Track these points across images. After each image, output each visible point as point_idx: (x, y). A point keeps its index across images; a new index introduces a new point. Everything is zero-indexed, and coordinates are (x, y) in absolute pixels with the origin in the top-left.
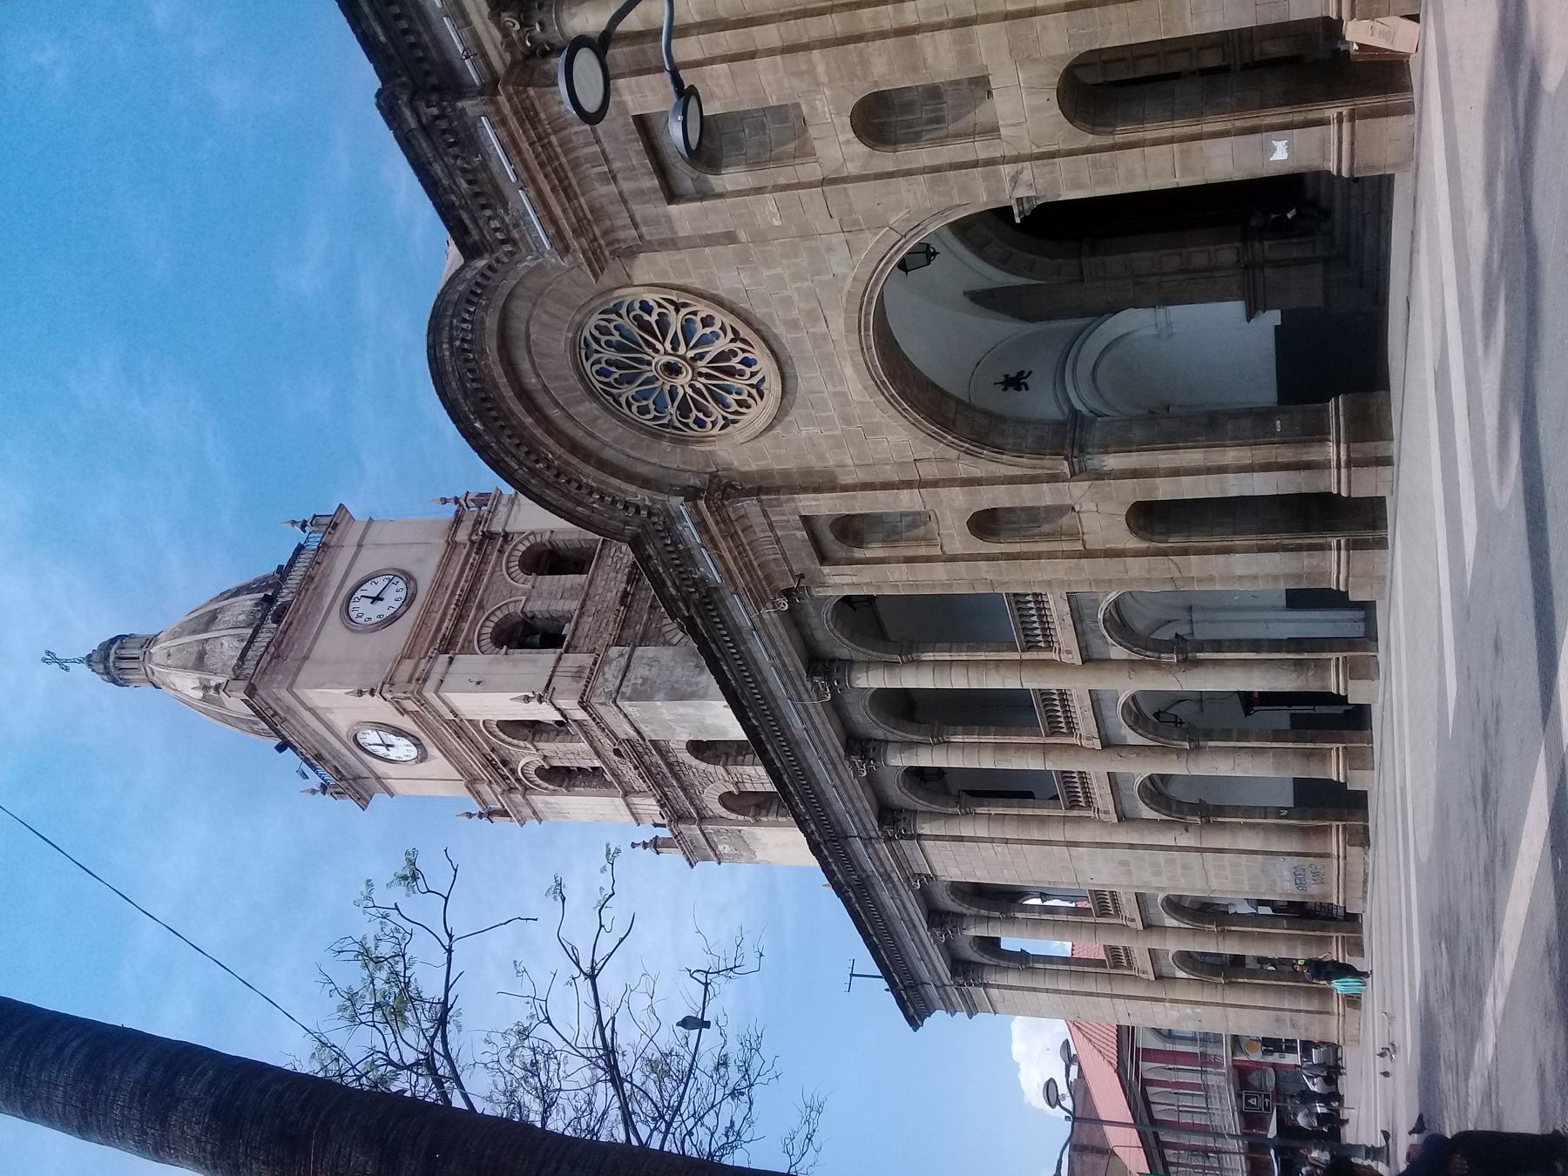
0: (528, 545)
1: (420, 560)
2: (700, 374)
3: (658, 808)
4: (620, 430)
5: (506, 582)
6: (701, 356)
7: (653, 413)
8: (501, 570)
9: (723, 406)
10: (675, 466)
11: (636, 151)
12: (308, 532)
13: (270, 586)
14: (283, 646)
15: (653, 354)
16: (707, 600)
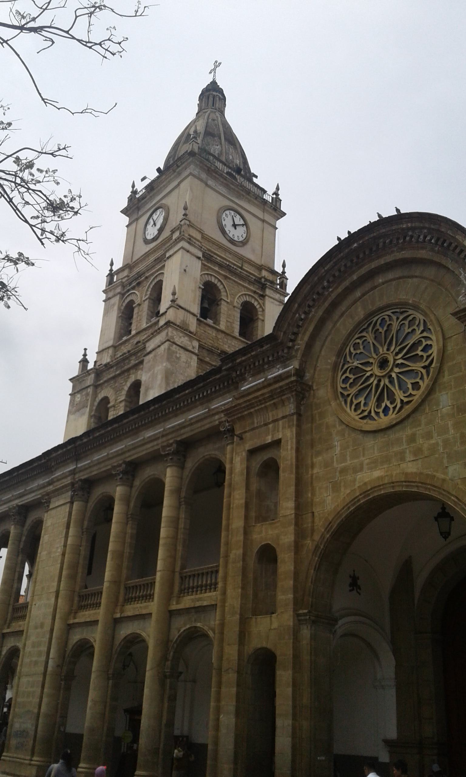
0: (258, 307)
2: (379, 381)
3: (104, 362)
5: (238, 293)
6: (391, 381)
7: (354, 352)
9: (357, 395)
10: (318, 365)
12: (273, 196)
13: (246, 174)
15: (394, 353)
16: (230, 382)
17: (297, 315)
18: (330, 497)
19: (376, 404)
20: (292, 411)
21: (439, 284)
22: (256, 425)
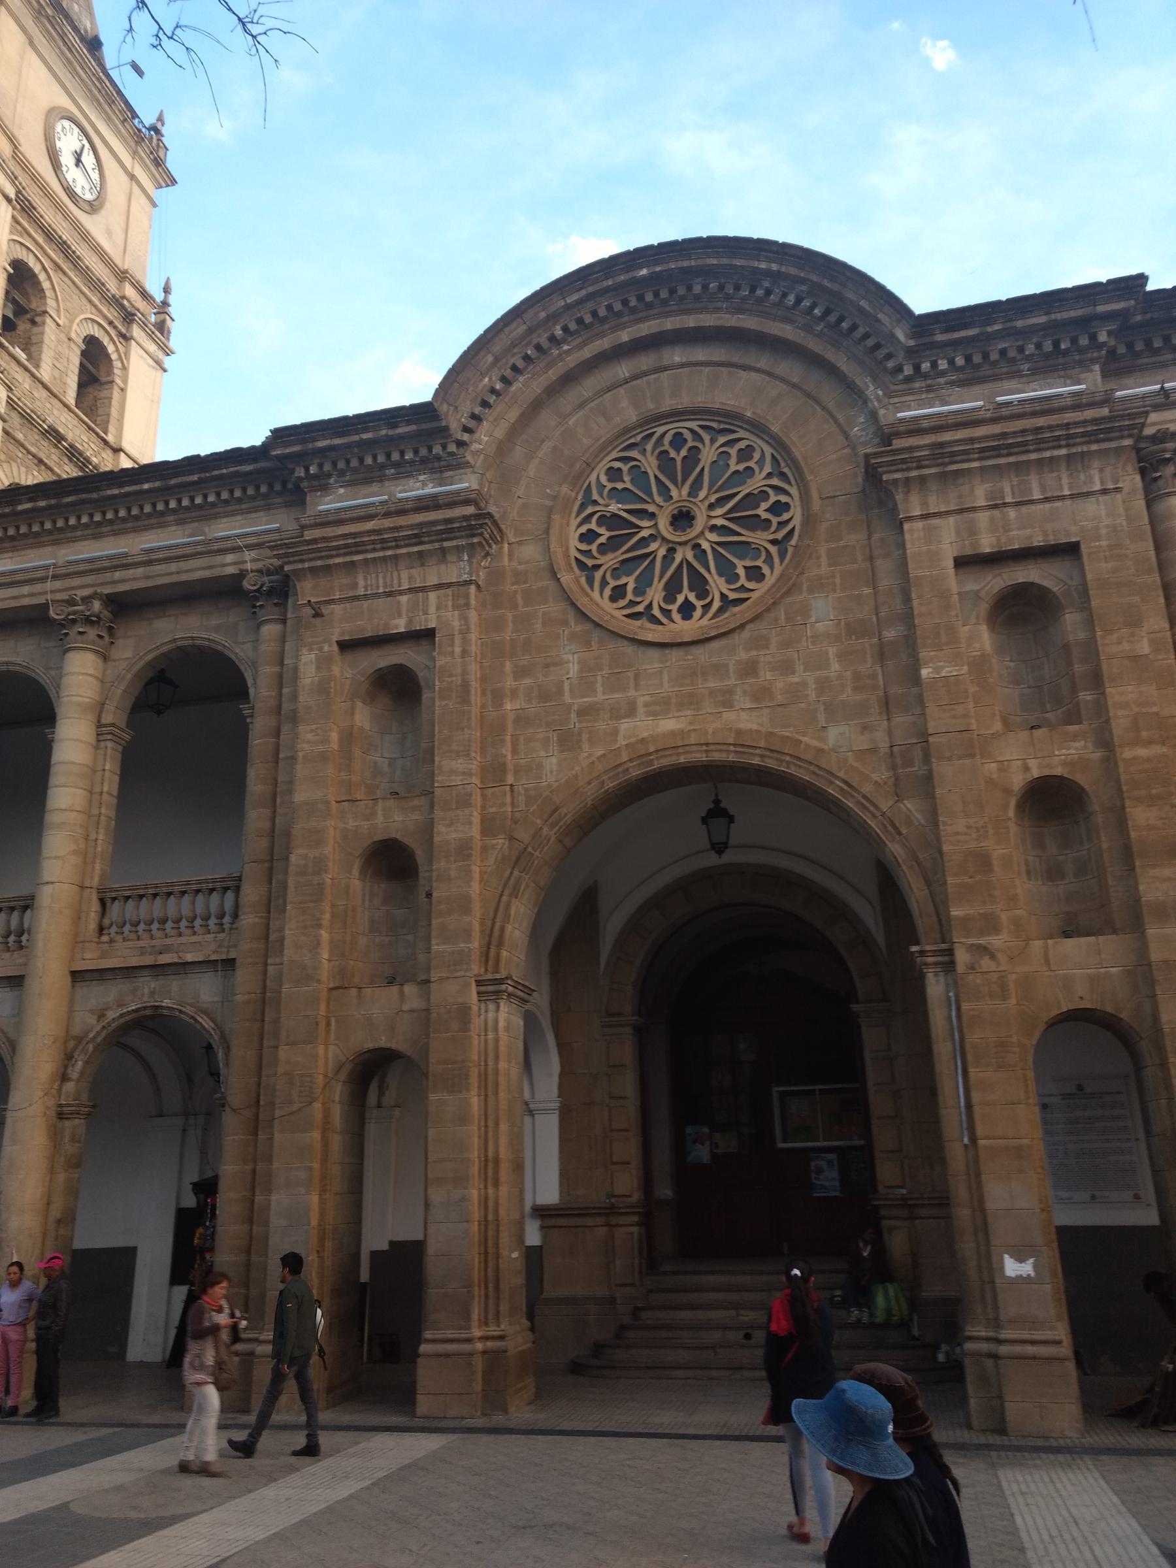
0: (114, 356)
1: (109, 232)
2: (672, 551)
4: (587, 442)
8: (92, 313)
11: (1030, 538)
14: (46, 23)
15: (707, 503)
16: (278, 487)
17: (487, 379)
19: (664, 593)
20: (465, 577)
22: (361, 592)
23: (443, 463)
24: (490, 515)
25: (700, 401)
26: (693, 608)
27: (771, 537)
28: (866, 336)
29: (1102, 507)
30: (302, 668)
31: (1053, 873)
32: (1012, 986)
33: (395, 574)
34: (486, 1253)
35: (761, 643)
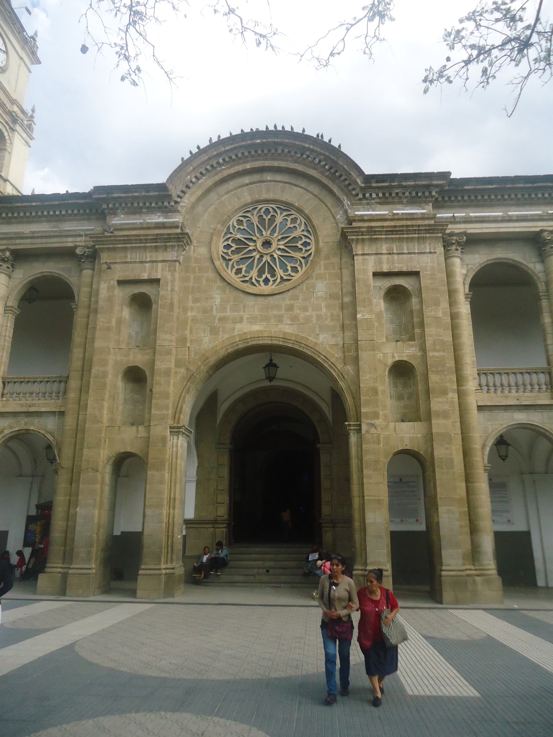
0: (7, 138)
2: (262, 256)
11: (402, 267)
15: (277, 239)
16: (94, 211)
17: (189, 177)
18: (207, 338)
19: (257, 274)
20: (175, 258)
21: (320, 200)
23: (168, 209)
24: (187, 234)
25: (278, 197)
26: (269, 281)
27: (302, 256)
28: (346, 180)
29: (429, 259)
30: (100, 290)
31: (400, 398)
32: (382, 439)
33: (144, 254)
34: (168, 536)
35: (296, 298)
